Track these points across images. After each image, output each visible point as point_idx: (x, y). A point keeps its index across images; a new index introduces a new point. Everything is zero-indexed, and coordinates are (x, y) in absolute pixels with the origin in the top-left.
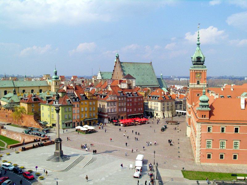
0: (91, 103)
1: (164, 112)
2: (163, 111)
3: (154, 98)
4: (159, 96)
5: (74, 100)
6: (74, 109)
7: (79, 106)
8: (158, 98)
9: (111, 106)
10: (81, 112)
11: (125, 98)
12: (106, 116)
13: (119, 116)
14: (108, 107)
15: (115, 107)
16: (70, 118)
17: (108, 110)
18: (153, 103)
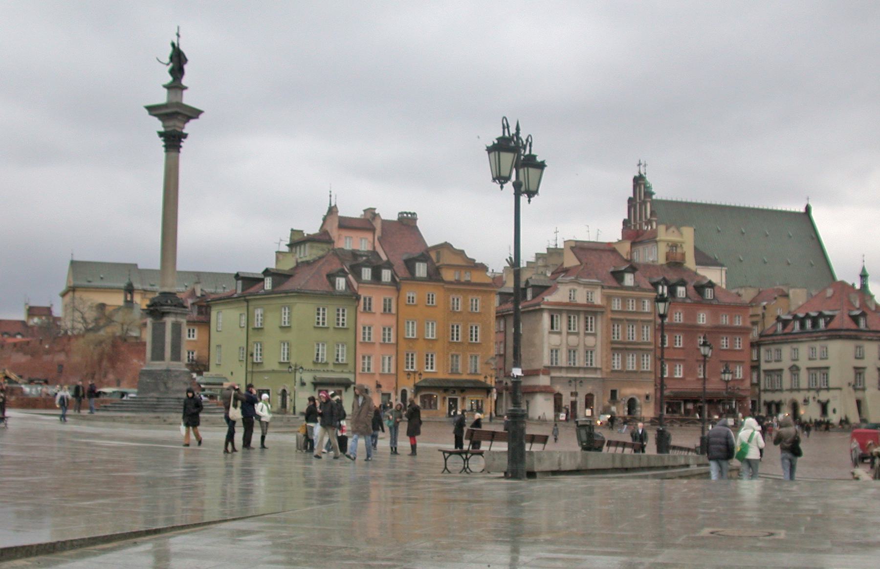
0: (460, 302)
1: (859, 395)
2: (855, 389)
3: (808, 324)
4: (836, 313)
6: (363, 320)
7: (394, 311)
8: (827, 324)
9: (569, 334)
10: (403, 345)
11: (647, 306)
12: (543, 381)
13: (614, 393)
14: (555, 340)
15: (590, 341)
16: (346, 364)
17: (554, 351)
18: (804, 349)
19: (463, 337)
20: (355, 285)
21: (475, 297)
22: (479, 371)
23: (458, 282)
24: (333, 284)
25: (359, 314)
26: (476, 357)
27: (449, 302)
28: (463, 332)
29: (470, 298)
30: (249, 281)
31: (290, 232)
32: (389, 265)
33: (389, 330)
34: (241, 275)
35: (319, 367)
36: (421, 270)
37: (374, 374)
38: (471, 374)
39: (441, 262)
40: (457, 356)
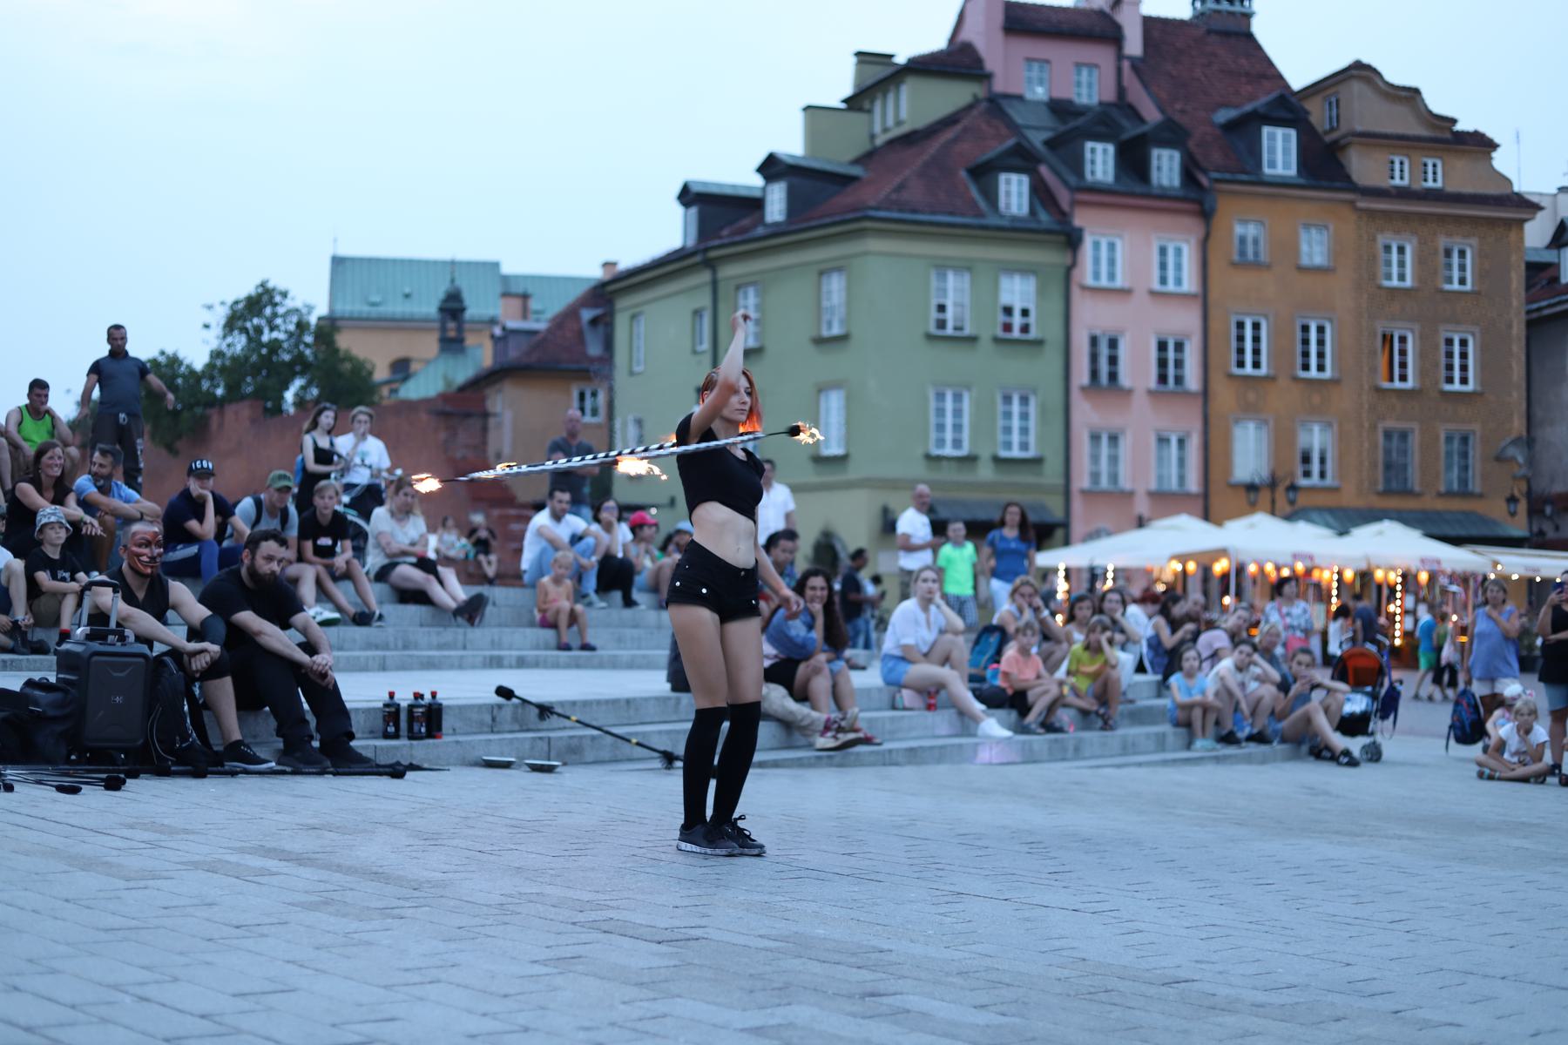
5: (1100, 161)
7: (1190, 284)
10: (1224, 395)
16: (1037, 462)
19: (1422, 373)
20: (1064, 197)
21: (1456, 243)
22: (1475, 486)
23: (1403, 194)
24: (991, 196)
25: (1076, 293)
26: (1465, 440)
27: (1373, 258)
28: (1422, 355)
29: (1442, 242)
30: (716, 212)
31: (854, 60)
32: (1171, 134)
33: (1179, 347)
34: (695, 189)
35: (948, 474)
36: (1280, 150)
37: (1129, 495)
38: (1450, 494)
39: (1344, 129)
40: (1404, 436)
